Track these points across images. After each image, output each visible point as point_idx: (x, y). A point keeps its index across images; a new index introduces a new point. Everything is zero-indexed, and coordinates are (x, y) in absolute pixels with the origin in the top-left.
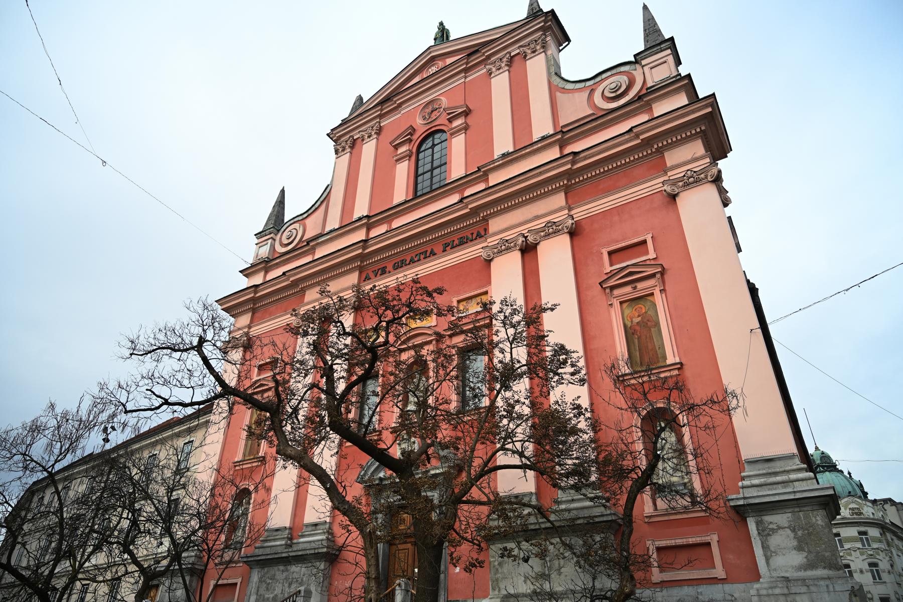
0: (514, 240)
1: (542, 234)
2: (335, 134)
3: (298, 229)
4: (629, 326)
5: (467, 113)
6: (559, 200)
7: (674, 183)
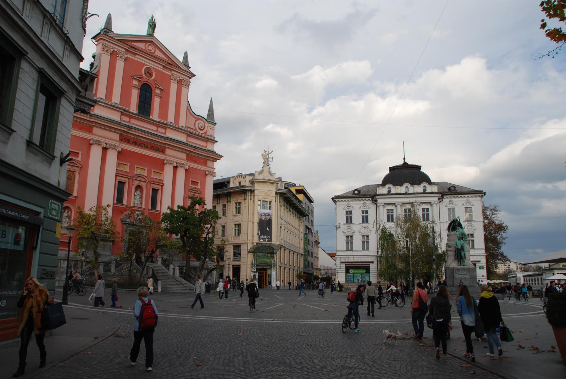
2: (104, 37)
5: (161, 90)
6: (184, 156)
7: (208, 172)
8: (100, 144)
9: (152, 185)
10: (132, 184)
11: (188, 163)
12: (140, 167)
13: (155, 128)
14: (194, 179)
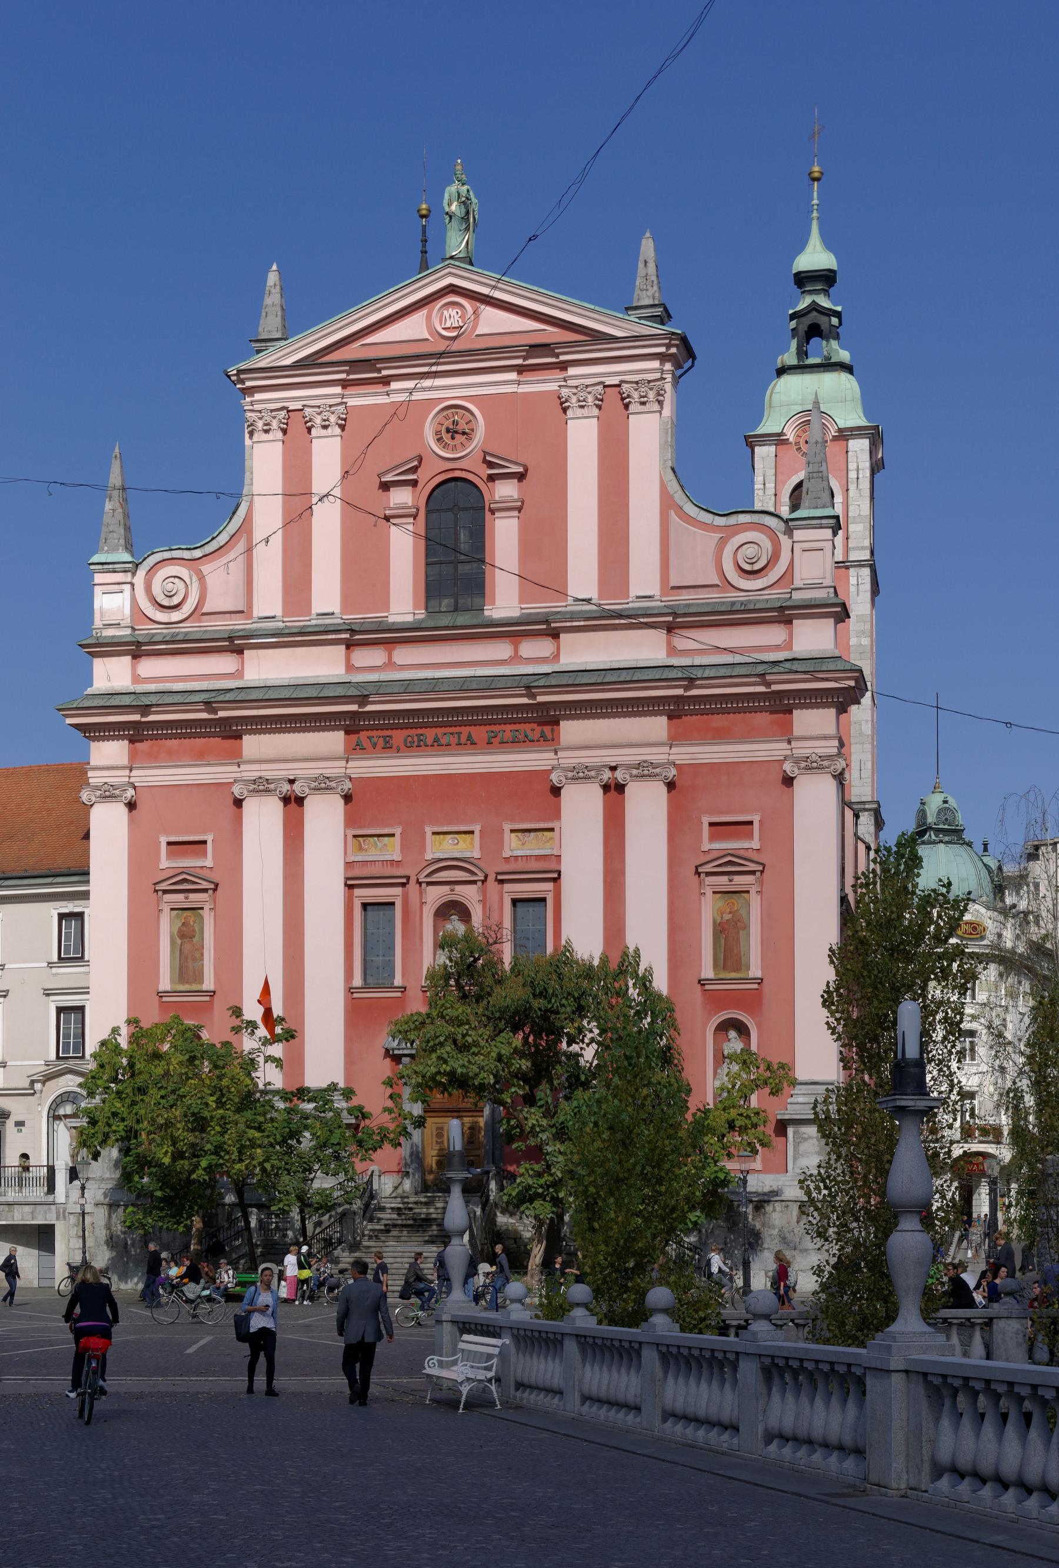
0: (599, 769)
1: (635, 772)
3: (188, 582)
4: (719, 920)
8: (267, 791)
9: (507, 887)
10: (422, 903)
11: (674, 750)
12: (445, 829)
13: (501, 650)
14: (722, 812)
